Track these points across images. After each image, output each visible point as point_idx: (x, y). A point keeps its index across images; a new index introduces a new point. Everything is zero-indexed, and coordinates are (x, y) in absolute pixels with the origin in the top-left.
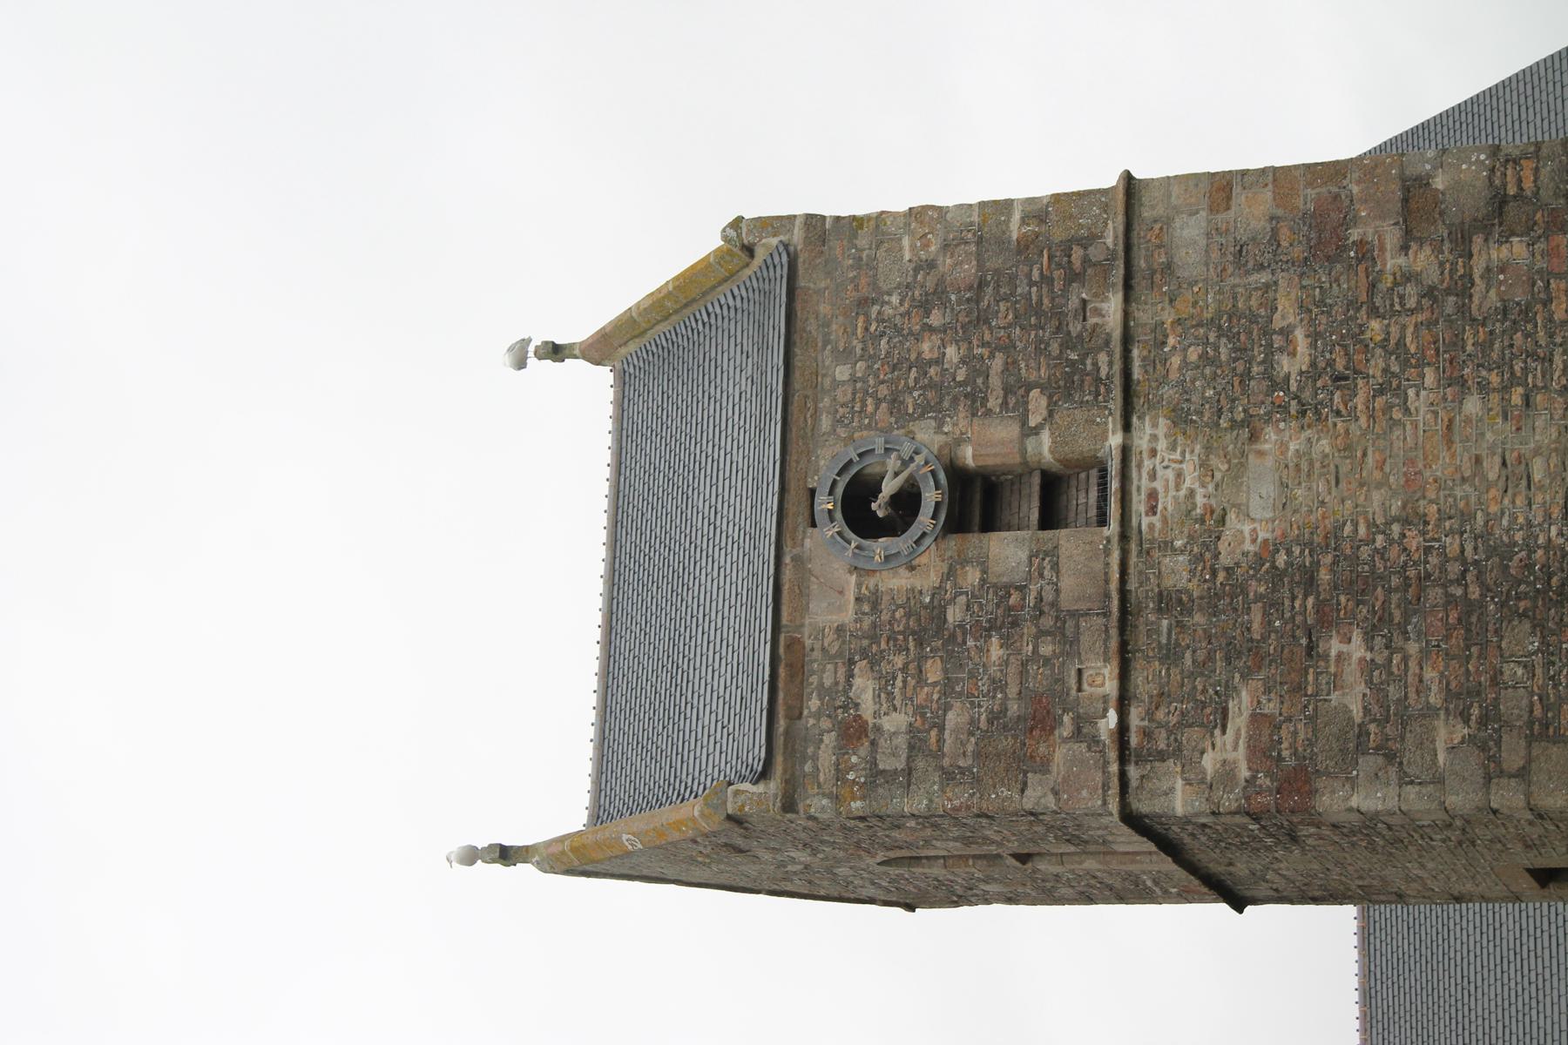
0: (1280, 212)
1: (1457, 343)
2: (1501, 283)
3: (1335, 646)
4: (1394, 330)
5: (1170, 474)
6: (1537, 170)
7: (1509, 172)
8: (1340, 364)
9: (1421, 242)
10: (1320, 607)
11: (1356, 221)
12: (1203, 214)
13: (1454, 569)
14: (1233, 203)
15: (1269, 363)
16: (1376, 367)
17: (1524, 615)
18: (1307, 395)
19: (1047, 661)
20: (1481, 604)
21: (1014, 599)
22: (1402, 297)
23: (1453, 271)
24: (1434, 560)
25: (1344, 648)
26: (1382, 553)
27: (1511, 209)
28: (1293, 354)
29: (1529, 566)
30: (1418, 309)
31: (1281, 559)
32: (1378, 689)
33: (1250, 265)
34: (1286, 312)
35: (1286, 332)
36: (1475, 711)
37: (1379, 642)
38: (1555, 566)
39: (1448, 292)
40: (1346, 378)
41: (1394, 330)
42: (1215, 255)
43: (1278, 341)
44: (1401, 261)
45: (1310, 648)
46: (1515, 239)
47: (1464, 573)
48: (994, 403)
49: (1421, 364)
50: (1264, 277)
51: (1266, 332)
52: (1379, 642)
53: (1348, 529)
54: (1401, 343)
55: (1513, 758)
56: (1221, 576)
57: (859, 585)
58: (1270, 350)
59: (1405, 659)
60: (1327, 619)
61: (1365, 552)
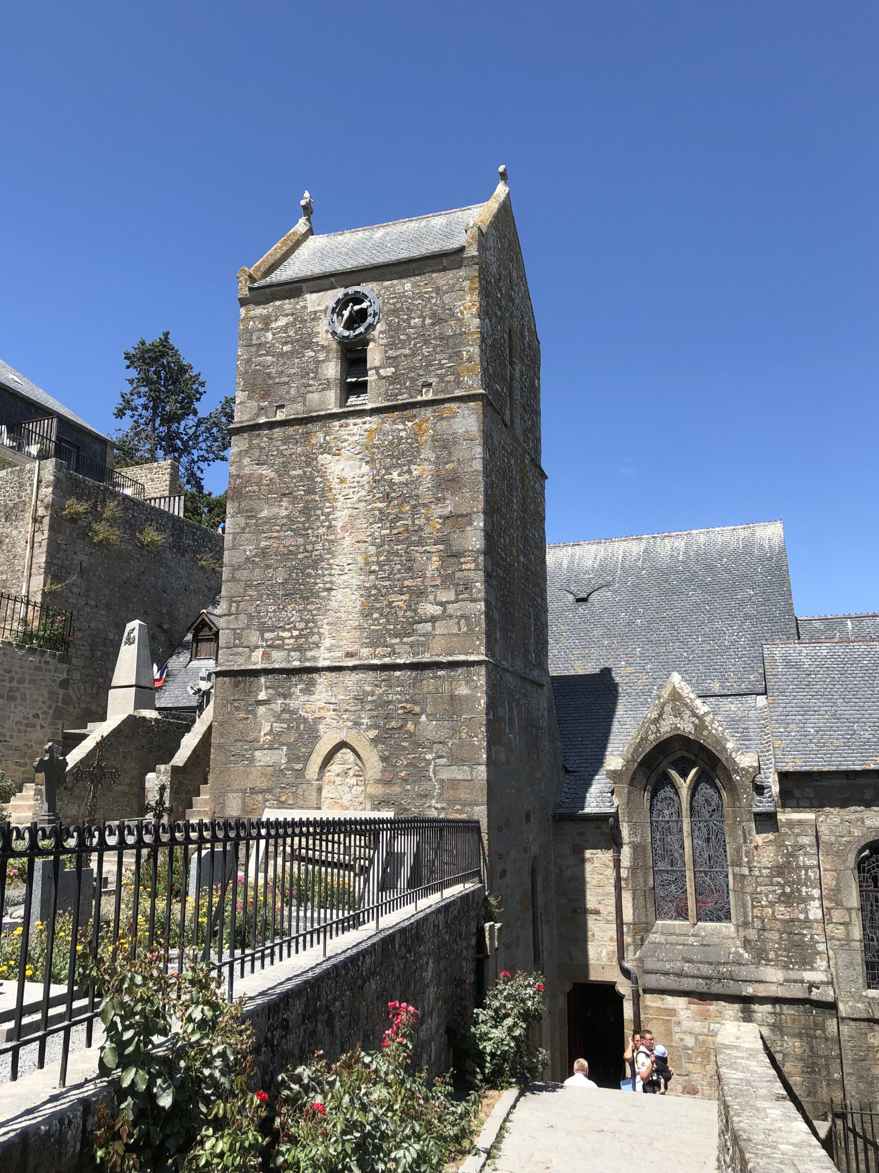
5: (355, 431)
8: (393, 495)
13: (309, 547)
17: (290, 575)
19: (288, 392)
21: (312, 375)
22: (419, 518)
23: (429, 538)
26: (318, 519)
28: (399, 475)
32: (268, 520)
36: (257, 559)
43: (405, 468)
45: (284, 495)
48: (390, 353)
49: (391, 528)
53: (328, 505)
54: (402, 519)
55: (238, 575)
57: (320, 311)
58: (401, 466)
59: (278, 531)
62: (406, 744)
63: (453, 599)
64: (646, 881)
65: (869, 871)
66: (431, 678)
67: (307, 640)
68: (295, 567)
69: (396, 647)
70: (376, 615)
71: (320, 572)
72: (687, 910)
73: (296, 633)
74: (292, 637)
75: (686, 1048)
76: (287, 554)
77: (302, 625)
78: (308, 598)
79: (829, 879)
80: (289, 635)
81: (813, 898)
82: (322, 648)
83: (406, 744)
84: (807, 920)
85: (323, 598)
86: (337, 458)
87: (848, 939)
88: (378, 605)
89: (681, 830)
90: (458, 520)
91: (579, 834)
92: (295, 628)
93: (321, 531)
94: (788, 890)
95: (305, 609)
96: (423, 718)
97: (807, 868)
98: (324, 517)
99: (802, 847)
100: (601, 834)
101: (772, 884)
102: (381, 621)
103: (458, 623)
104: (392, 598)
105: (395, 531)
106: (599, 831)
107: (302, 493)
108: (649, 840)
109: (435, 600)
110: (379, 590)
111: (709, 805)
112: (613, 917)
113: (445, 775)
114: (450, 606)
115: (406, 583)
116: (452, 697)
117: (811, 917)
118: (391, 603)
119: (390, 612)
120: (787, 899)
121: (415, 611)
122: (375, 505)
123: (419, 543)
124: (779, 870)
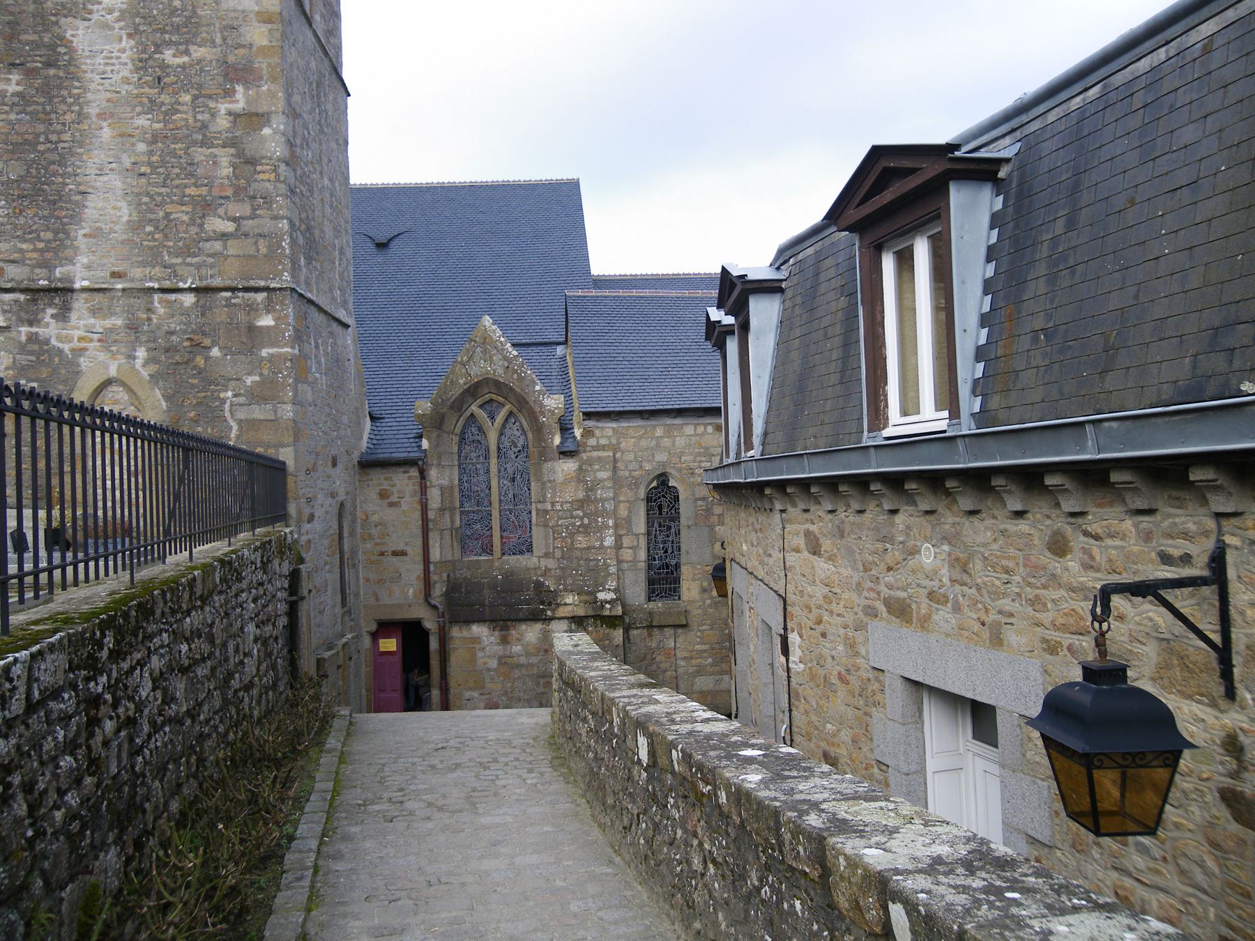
0: (254, 49)
1: (176, 140)
2: (208, 162)
3: (15, 77)
4: (184, 108)
6: (269, 181)
7: (269, 167)
8: (166, 80)
9: (235, 122)
10: (35, 70)
11: (247, 89)
12: (256, 8)
13: (54, 138)
14: (262, 24)
15: (169, 44)
16: (165, 98)
17: (28, 172)
18: (151, 63)
20: (35, 150)
22: (203, 112)
23: (216, 138)
24: (59, 127)
25: (14, 82)
26: (64, 101)
27: (249, 168)
28: (174, 56)
29: (54, 175)
30: (196, 121)
31: (62, 50)
33: (226, 33)
34: (198, 52)
35: (187, 52)
37: (16, 100)
38: (54, 187)
39: (204, 135)
40: (159, 83)
41: (184, 108)
42: (232, 15)
43: (182, 47)
44: (223, 112)
45: (14, 65)
46: (231, 169)
47: (50, 142)
49: (166, 122)
50: (219, 40)
51: (187, 42)
52: (16, 100)
53: (77, 84)
54: (177, 111)
56: (53, 19)
58: (177, 44)
59: (7, 113)
60: (30, 73)
61: (65, 93)
62: (195, 381)
63: (248, 214)
64: (452, 522)
65: (655, 500)
66: (225, 306)
67: (56, 254)
68: (34, 161)
69: (177, 268)
70: (149, 229)
71: (69, 169)
72: (492, 546)
73: (41, 245)
74: (35, 250)
75: (489, 670)
76: (21, 144)
77: (49, 235)
78: (55, 202)
79: (623, 511)
80: (31, 247)
81: (608, 527)
82: (78, 265)
83: (195, 381)
84: (602, 546)
85: (76, 203)
86: (87, 23)
87: (635, 561)
88: (153, 216)
89: (488, 471)
90: (252, 119)
91: (386, 479)
92: (39, 239)
93: (69, 117)
94: (586, 521)
95: (52, 216)
96: (215, 352)
97: (603, 500)
98: (72, 100)
99: (601, 481)
100: (409, 478)
101: (572, 517)
102: (157, 236)
103: (256, 243)
104: (169, 208)
105: (171, 126)
106: (407, 475)
107: (39, 65)
108: (456, 482)
109: (226, 213)
110: (152, 197)
111: (516, 446)
112: (419, 558)
113: (241, 415)
114: (245, 222)
115: (188, 191)
116: (252, 329)
117: (605, 544)
118: (168, 214)
119: (167, 226)
120: (586, 530)
121: (201, 225)
122: (143, 90)
123: (203, 144)
124: (581, 504)
